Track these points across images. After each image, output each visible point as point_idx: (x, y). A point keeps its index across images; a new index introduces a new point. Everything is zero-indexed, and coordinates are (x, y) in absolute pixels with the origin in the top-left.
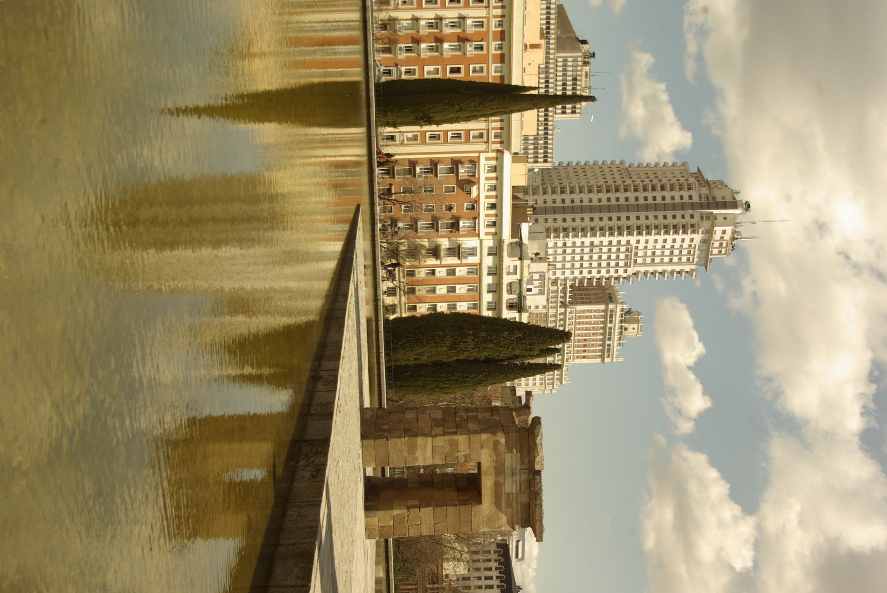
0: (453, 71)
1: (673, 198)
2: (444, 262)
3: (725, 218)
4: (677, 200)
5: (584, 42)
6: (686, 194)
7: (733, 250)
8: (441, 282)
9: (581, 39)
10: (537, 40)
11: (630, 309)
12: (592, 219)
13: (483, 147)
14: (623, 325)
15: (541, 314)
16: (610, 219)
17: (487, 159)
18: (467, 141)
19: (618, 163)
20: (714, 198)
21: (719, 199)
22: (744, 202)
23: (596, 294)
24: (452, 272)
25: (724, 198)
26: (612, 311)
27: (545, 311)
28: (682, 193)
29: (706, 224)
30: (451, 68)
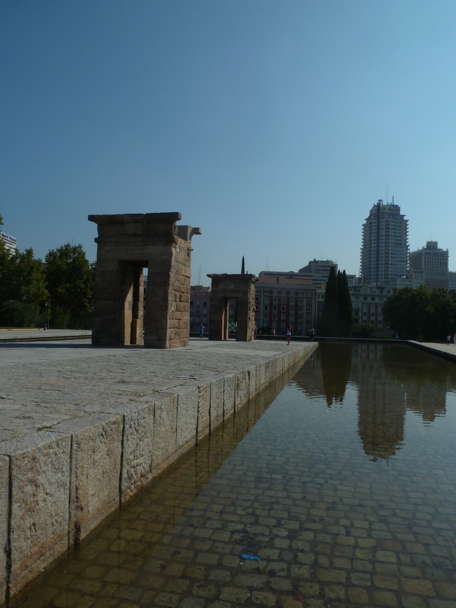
0: (283, 309)
1: (375, 229)
2: (361, 317)
3: (384, 209)
4: (376, 228)
6: (374, 224)
7: (398, 206)
8: (369, 318)
9: (308, 264)
10: (276, 279)
11: (426, 246)
13: (313, 300)
14: (432, 248)
15: (425, 282)
17: (319, 298)
18: (311, 305)
19: (361, 251)
20: (376, 214)
21: (376, 212)
23: (418, 259)
25: (376, 210)
26: (426, 253)
27: (424, 280)
28: (373, 226)
29: (386, 216)
30: (283, 310)
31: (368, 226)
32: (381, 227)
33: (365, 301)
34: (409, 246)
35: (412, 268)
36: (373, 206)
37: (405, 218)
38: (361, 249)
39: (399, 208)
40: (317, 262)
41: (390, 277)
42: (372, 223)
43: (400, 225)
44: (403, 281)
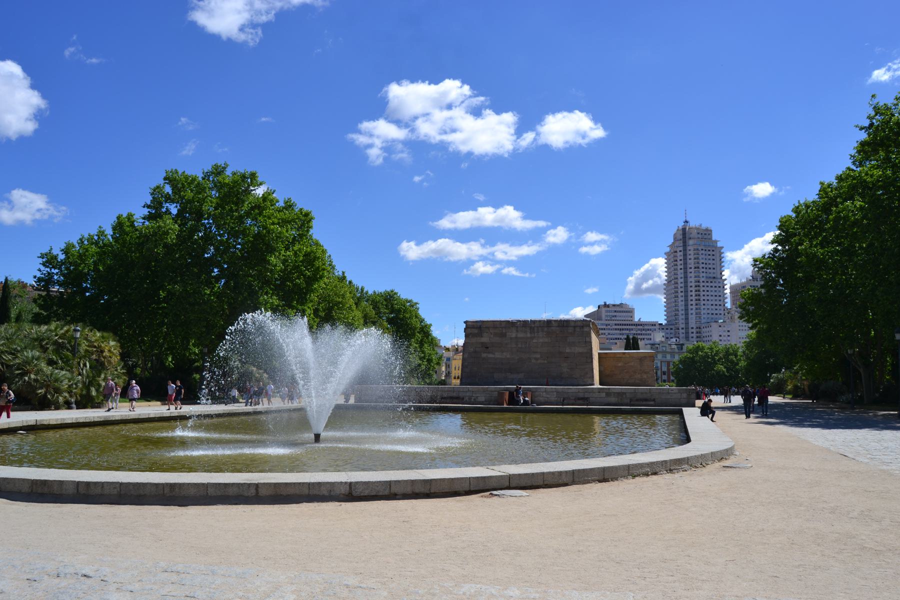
5: (599, 307)
9: (597, 308)
12: (692, 300)
14: (759, 280)
16: (691, 291)
21: (681, 237)
22: (684, 224)
24: (664, 373)
25: (681, 235)
31: (672, 256)
32: (689, 257)
33: (664, 359)
34: (726, 280)
35: (734, 306)
36: (676, 228)
37: (719, 245)
38: (665, 284)
39: (711, 231)
40: (608, 306)
41: (703, 321)
42: (676, 252)
43: (713, 253)
44: (720, 326)
